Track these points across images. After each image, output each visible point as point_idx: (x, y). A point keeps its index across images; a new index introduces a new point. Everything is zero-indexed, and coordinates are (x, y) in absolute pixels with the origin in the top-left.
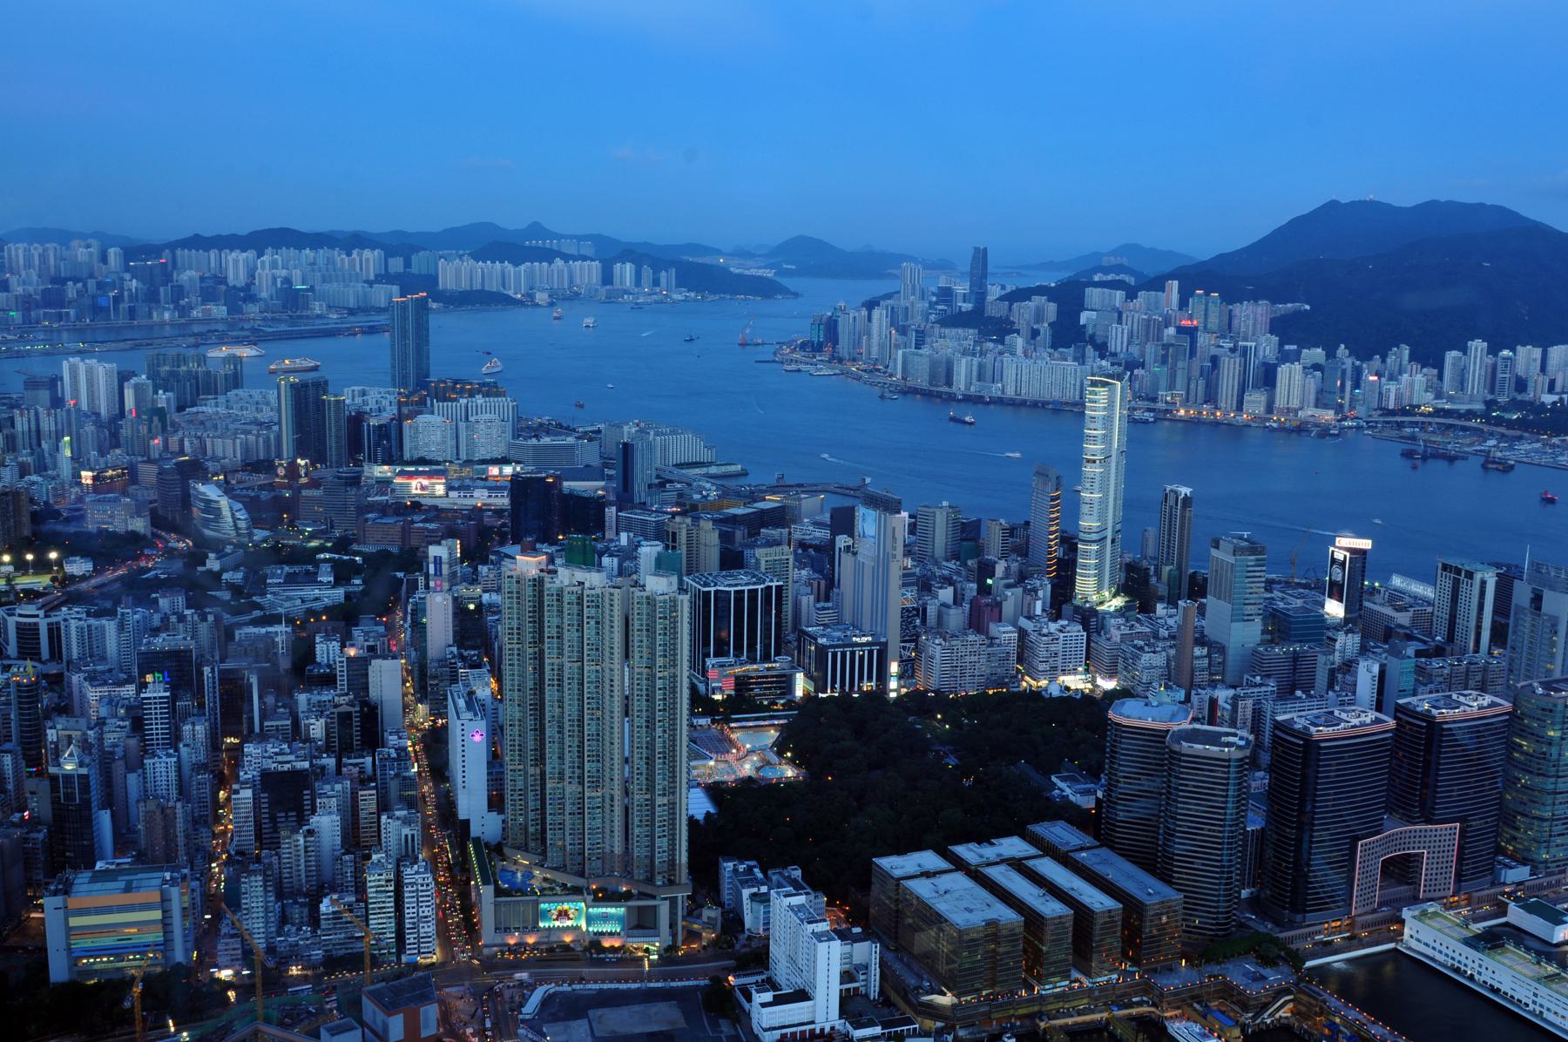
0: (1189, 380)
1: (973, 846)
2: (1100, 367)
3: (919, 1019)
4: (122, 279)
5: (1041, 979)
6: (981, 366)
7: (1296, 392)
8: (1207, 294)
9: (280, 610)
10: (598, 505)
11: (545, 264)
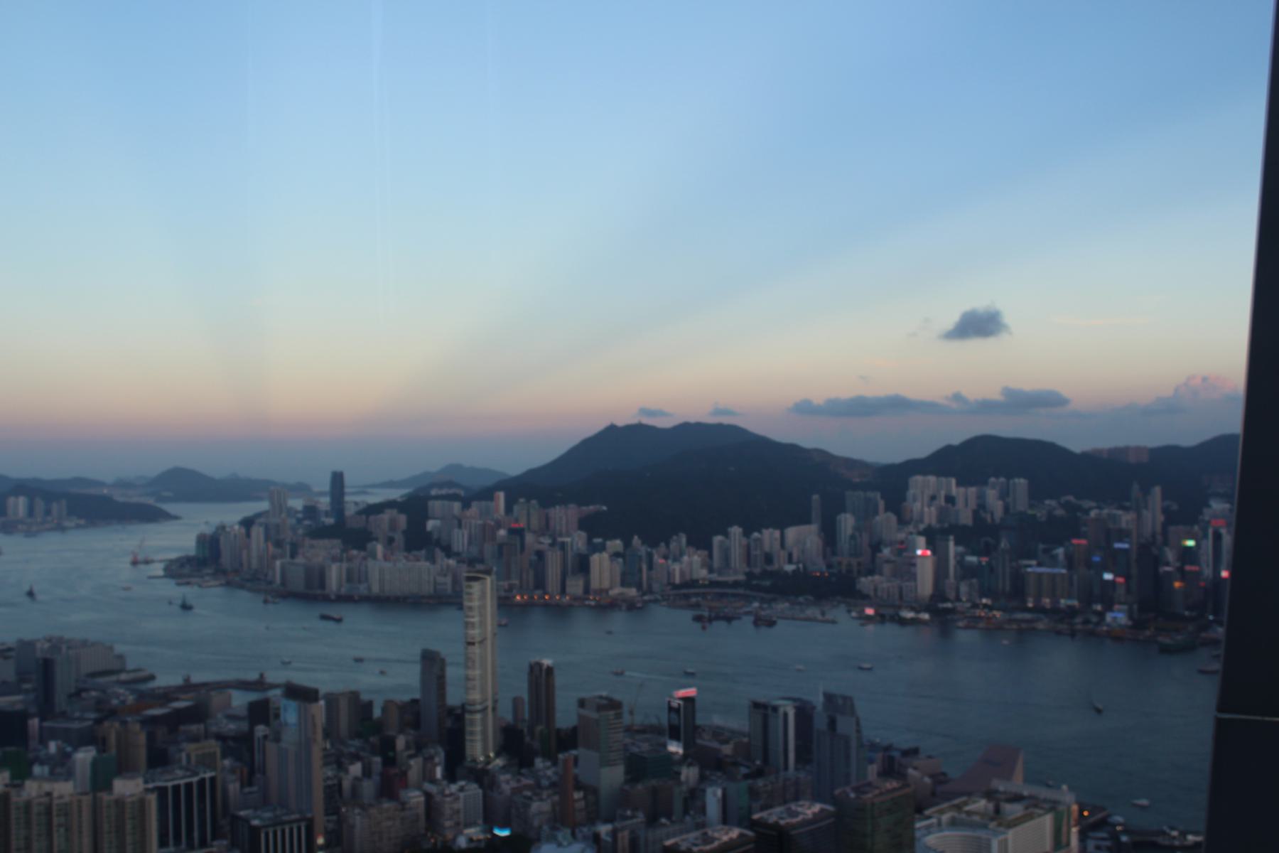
2: (448, 566)
6: (349, 572)
8: (528, 501)
10: (23, 717)
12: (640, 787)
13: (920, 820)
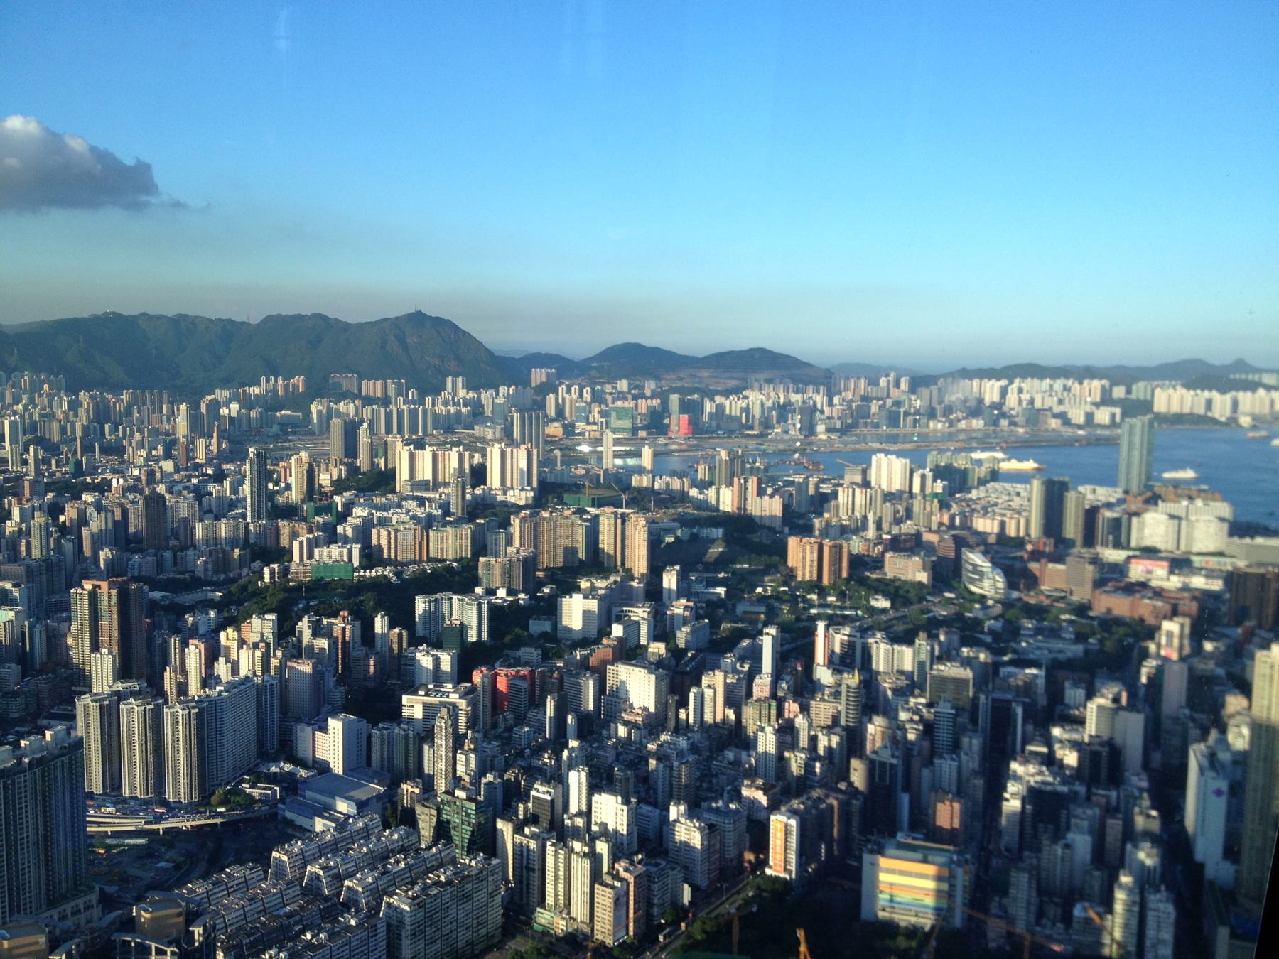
4: (910, 400)
9: (1032, 656)
11: (1249, 394)
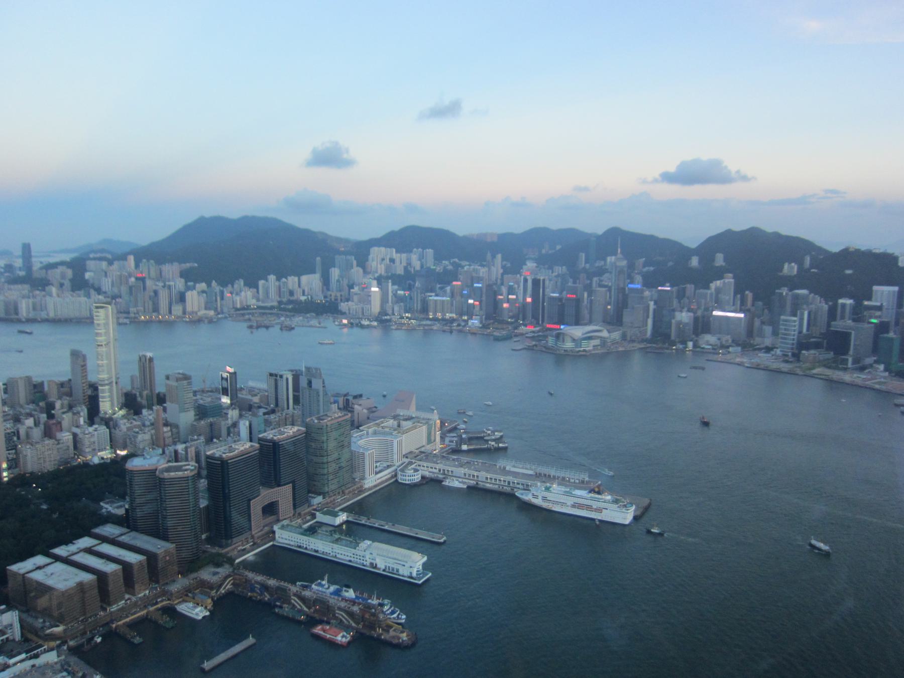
0: (144, 302)
1: (63, 547)
2: (98, 299)
3: (46, 643)
5: (110, 604)
7: (196, 304)
12: (202, 422)
13: (357, 432)
